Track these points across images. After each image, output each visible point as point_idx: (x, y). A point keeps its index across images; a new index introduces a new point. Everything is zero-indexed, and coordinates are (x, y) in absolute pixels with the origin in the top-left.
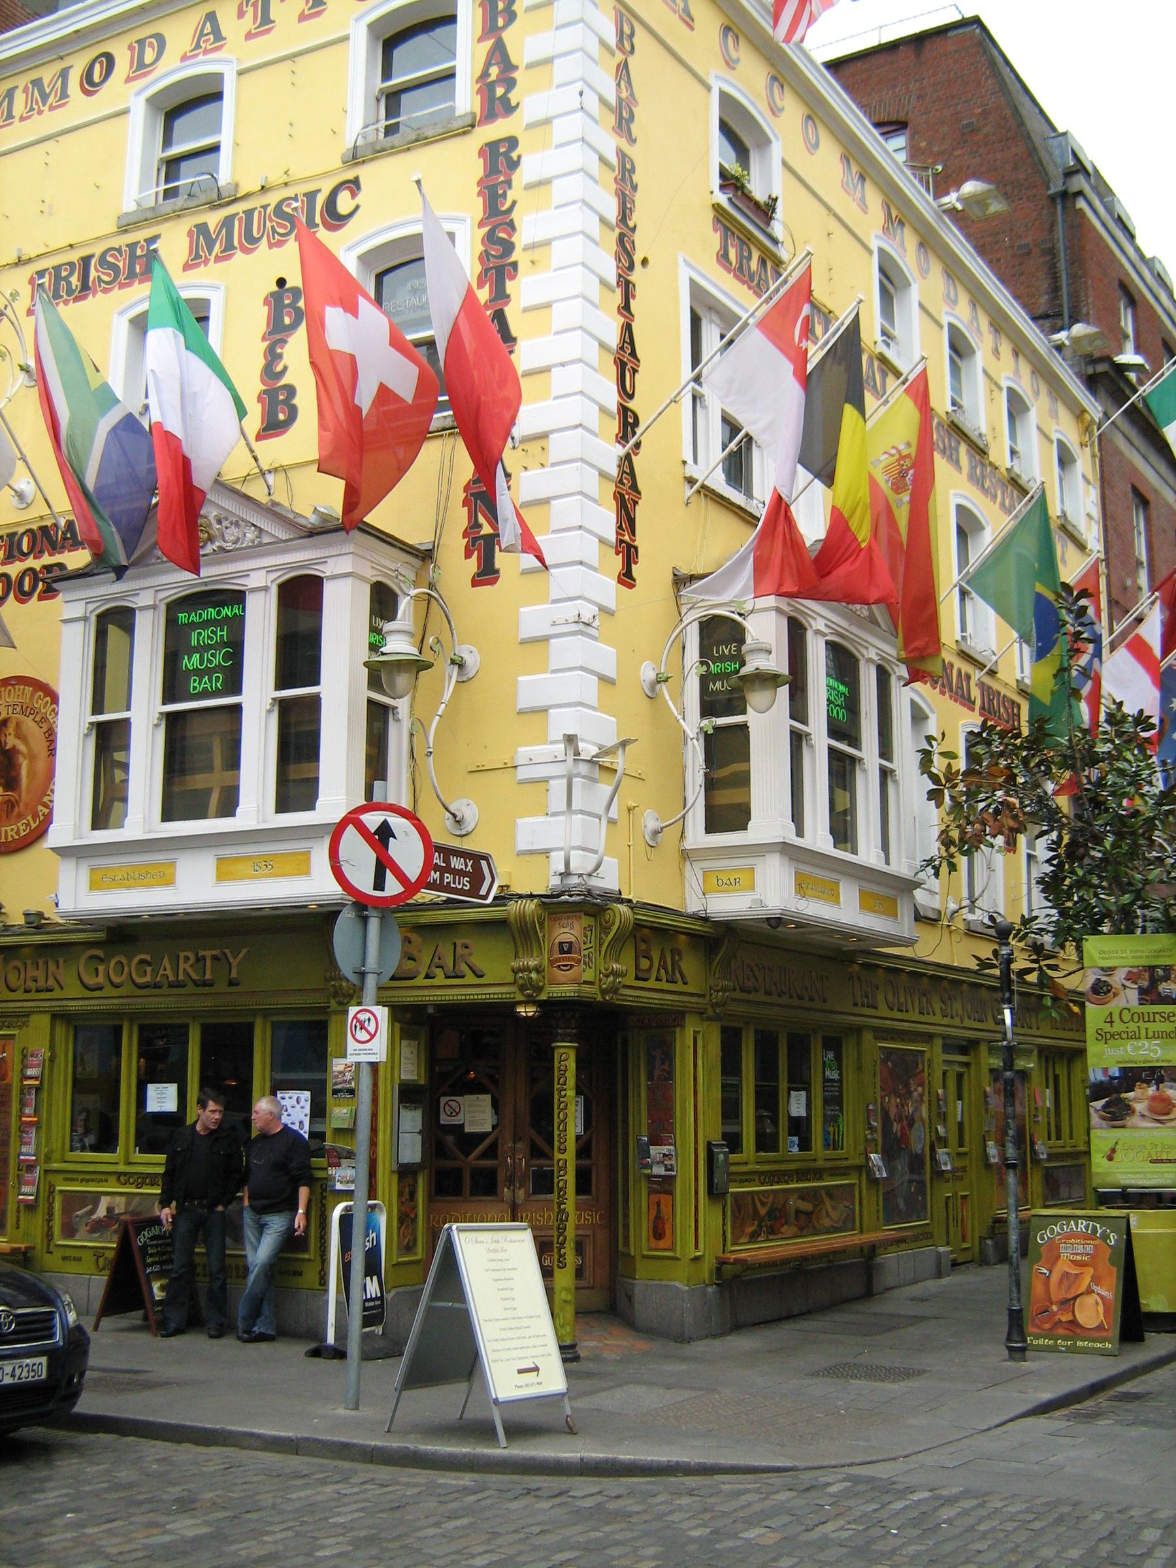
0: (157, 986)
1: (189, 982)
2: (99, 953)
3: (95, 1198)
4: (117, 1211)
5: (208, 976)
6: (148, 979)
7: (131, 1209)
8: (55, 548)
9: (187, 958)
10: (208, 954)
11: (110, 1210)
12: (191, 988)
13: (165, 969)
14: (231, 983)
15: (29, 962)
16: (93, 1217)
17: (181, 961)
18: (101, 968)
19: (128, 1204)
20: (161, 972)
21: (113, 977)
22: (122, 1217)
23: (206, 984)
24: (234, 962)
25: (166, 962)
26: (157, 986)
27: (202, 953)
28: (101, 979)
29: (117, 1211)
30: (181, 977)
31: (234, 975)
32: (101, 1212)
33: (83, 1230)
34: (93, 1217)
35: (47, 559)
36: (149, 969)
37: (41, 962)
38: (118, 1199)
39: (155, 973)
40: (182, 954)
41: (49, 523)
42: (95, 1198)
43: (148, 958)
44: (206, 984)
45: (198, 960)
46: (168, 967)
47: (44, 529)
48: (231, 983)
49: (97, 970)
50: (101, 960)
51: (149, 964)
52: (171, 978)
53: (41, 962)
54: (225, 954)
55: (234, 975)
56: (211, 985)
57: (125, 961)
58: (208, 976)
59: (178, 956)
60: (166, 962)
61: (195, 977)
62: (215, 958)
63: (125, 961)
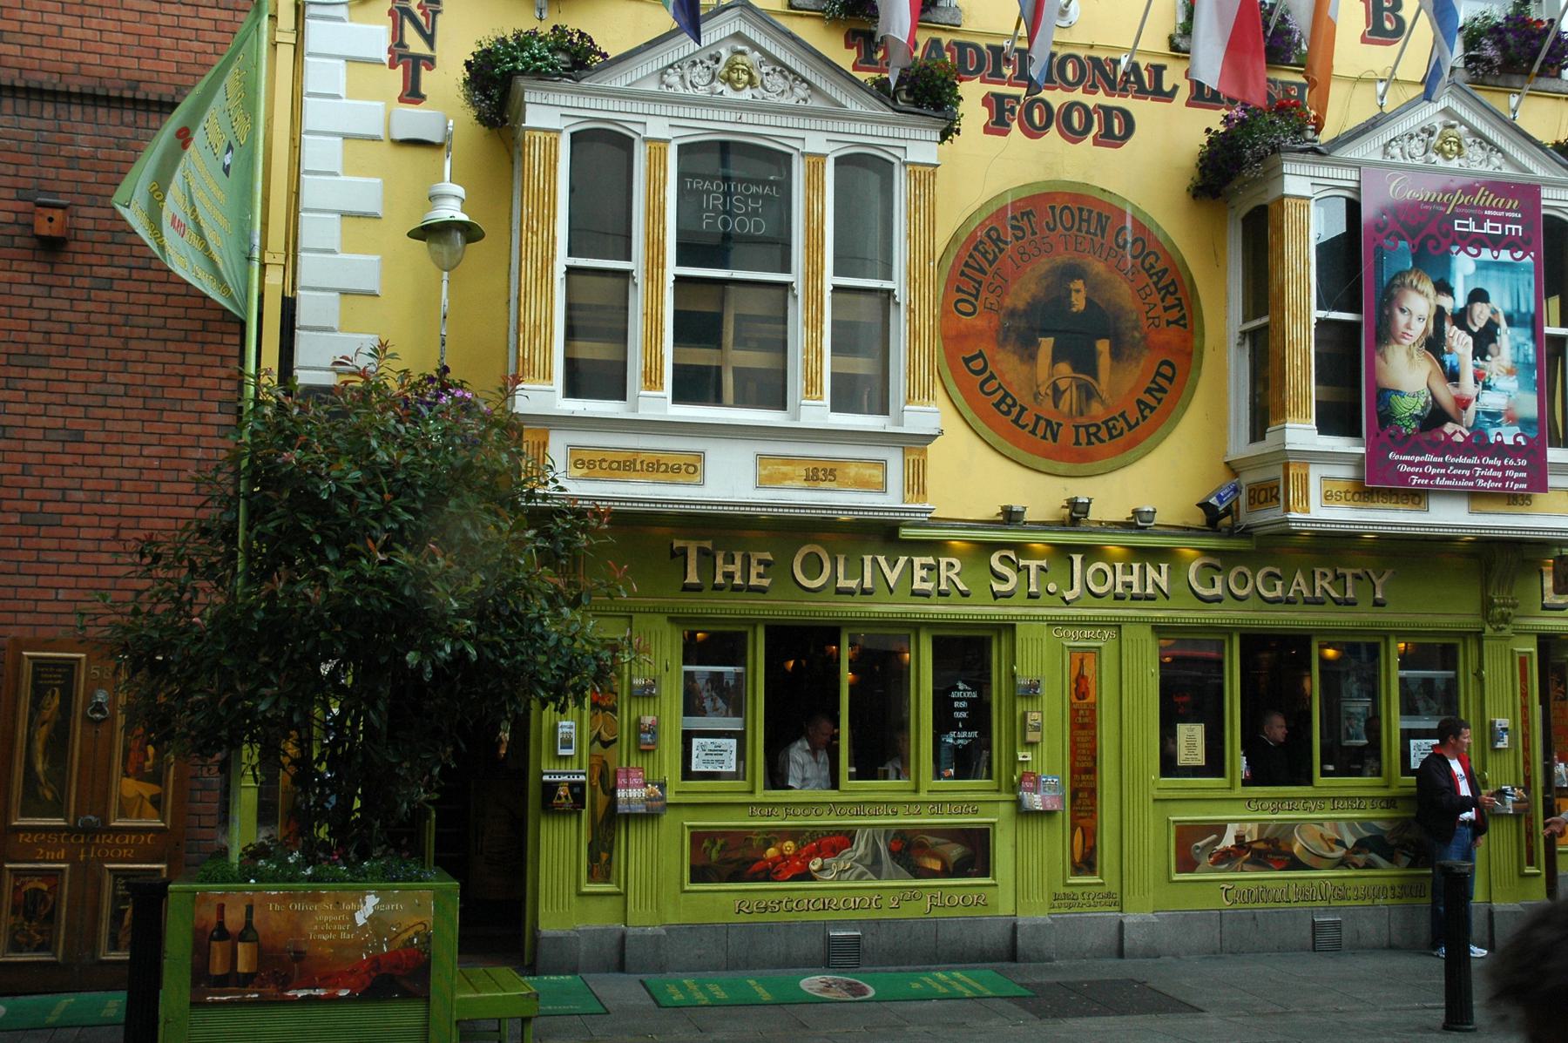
0: (1289, 601)
1: (1326, 598)
2: (1217, 562)
3: (1219, 829)
4: (1248, 839)
5: (1350, 594)
6: (1279, 592)
7: (1264, 837)
8: (1112, 87)
9: (1324, 575)
10: (1349, 572)
11: (1239, 838)
12: (1330, 605)
13: (1298, 585)
14: (1377, 603)
15: (1119, 566)
16: (1218, 848)
17: (1317, 576)
18: (1218, 579)
19: (1262, 829)
20: (1294, 587)
21: (1232, 586)
22: (1254, 846)
23: (1347, 603)
24: (1378, 583)
25: (1299, 577)
26: (1289, 601)
27: (1339, 571)
28: (1218, 590)
29: (1248, 839)
30: (1318, 593)
31: (1379, 596)
32: (1229, 841)
33: (1206, 861)
34: (1218, 848)
35: (1101, 98)
36: (1279, 584)
37: (1136, 566)
38: (1249, 825)
39: (1286, 588)
40: (1318, 572)
41: (1103, 56)
42: (1219, 829)
43: (1277, 571)
44: (1347, 603)
45: (1337, 577)
46: (1302, 581)
47: (1096, 62)
48: (1377, 603)
49: (1213, 580)
50: (1218, 569)
51: (1279, 578)
52: (1306, 594)
53: (1136, 566)
54: (1367, 573)
55: (1379, 596)
56: (1355, 604)
57: (1249, 574)
58: (1350, 594)
59: (1313, 572)
60: (1299, 577)
61: (1334, 594)
62: (1357, 577)
63: (1249, 574)
